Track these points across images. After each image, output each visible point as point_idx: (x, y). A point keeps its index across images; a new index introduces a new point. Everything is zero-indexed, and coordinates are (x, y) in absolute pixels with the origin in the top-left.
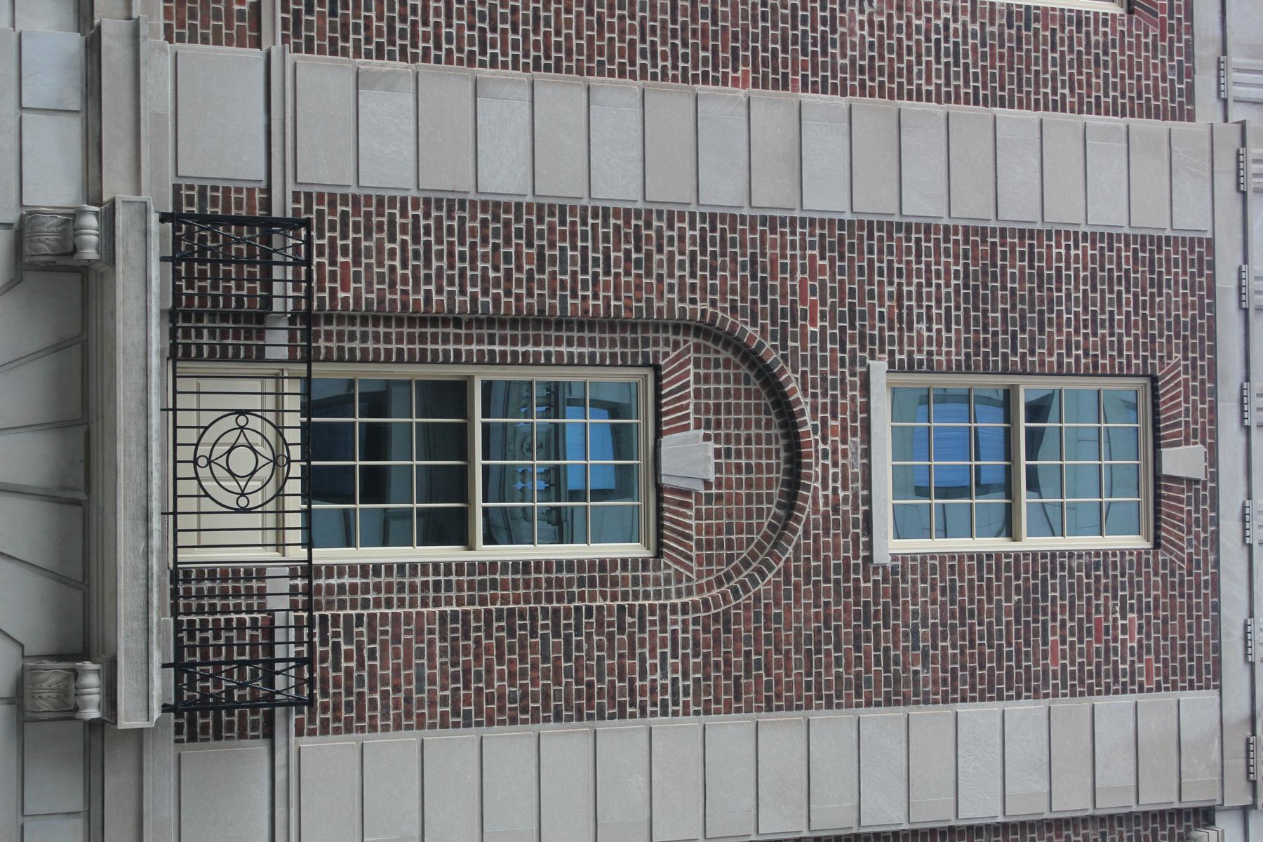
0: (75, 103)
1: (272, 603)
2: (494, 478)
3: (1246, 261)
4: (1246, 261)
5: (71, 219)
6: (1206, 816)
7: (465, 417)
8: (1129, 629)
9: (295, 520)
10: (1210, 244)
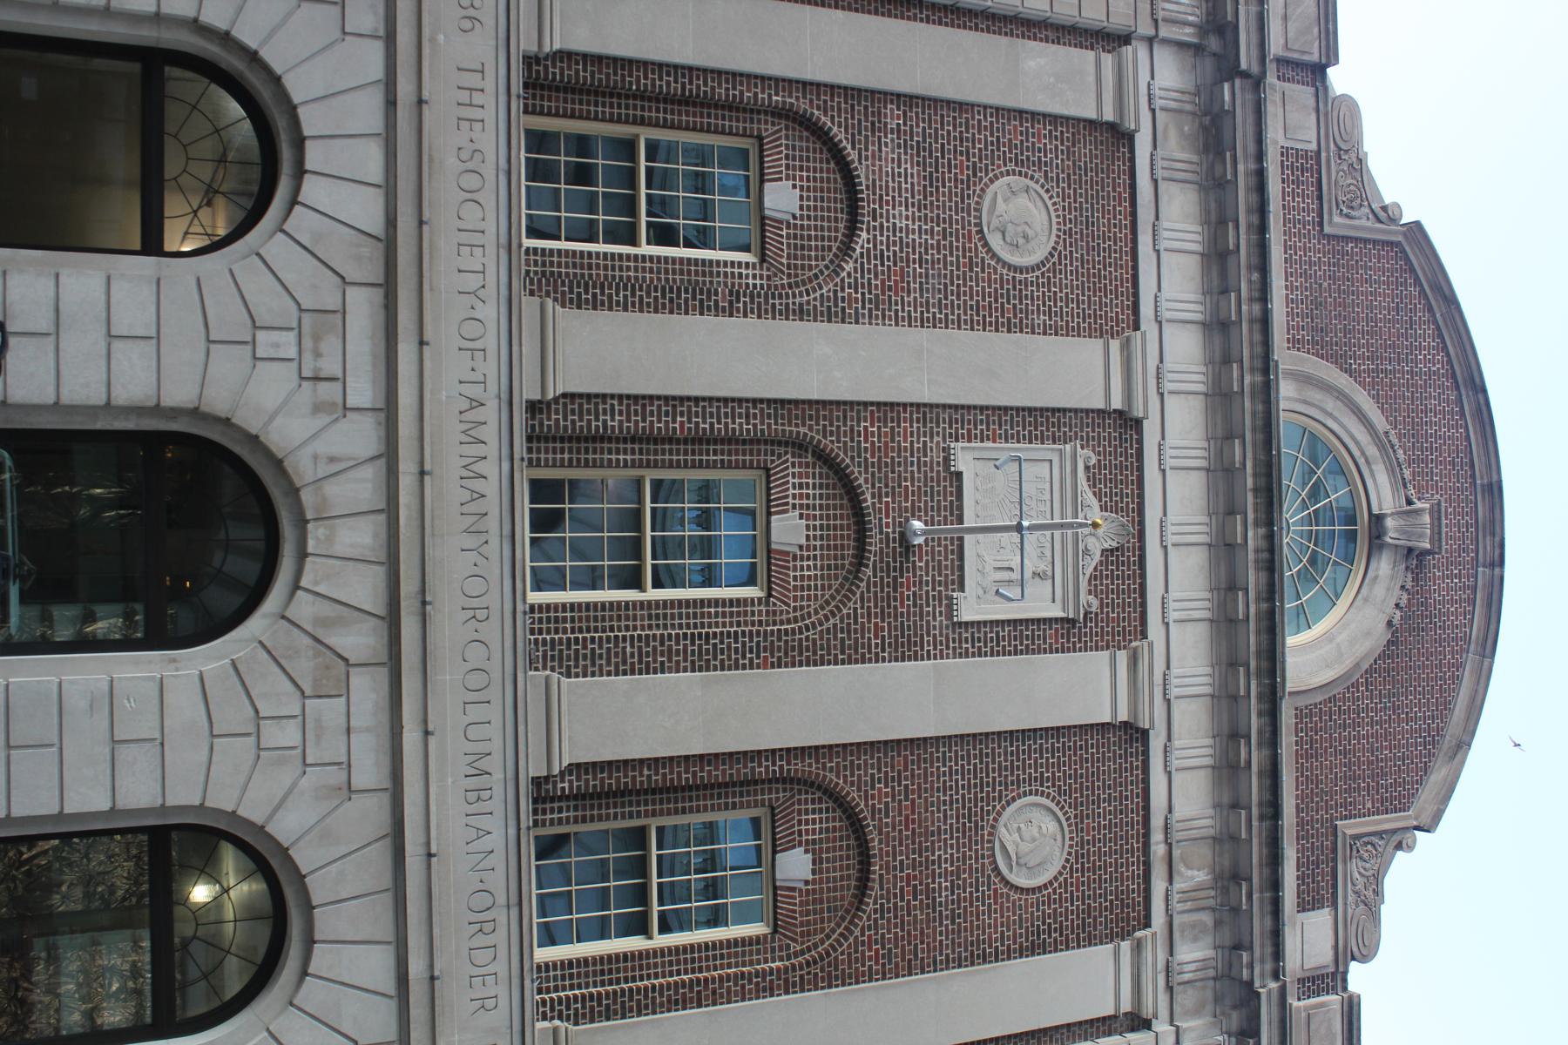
6: (1125, 39)
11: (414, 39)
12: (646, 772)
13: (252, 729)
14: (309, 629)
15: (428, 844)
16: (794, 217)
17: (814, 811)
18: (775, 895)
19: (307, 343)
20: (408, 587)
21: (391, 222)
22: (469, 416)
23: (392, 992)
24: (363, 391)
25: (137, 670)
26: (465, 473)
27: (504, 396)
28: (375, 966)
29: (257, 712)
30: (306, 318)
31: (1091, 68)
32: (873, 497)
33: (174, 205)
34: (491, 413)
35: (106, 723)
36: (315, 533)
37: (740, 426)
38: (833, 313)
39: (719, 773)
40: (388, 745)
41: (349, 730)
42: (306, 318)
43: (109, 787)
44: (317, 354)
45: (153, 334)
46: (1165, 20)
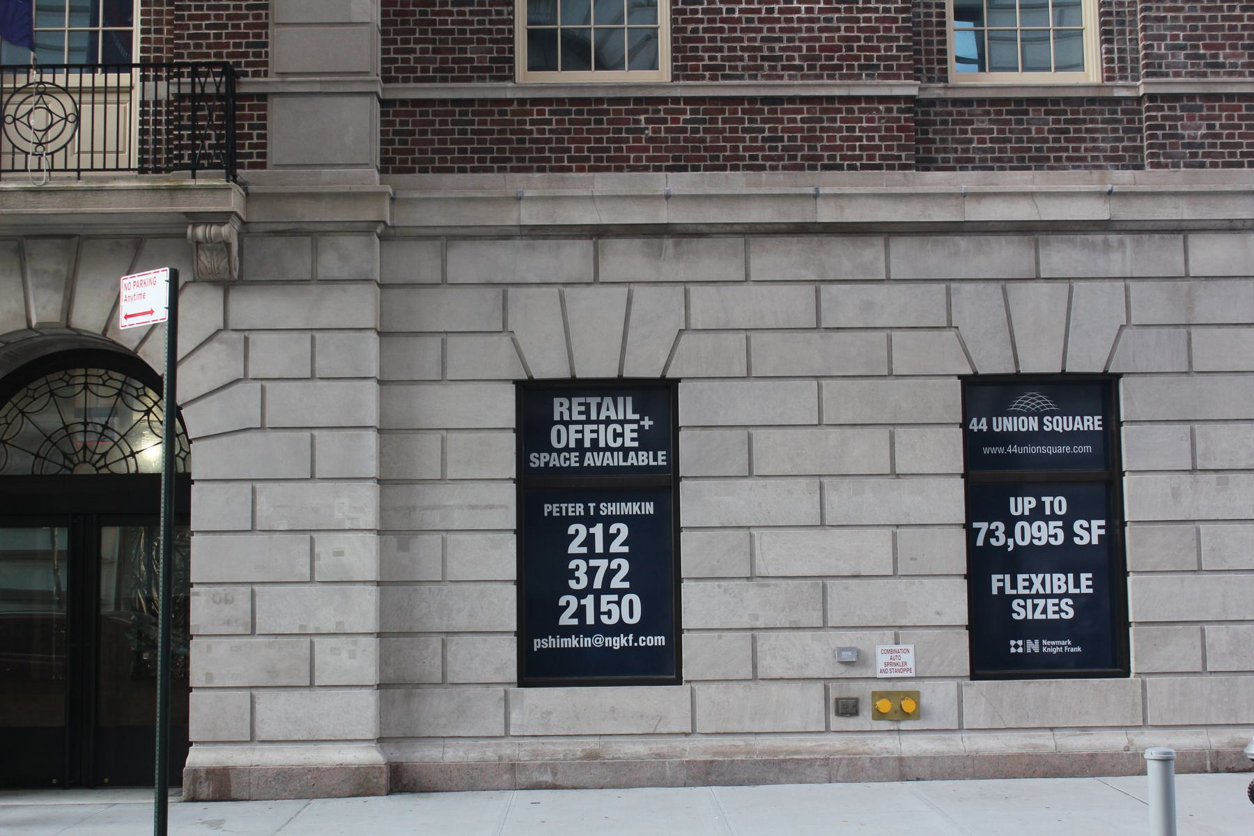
1: (162, 95)
9: (112, 79)
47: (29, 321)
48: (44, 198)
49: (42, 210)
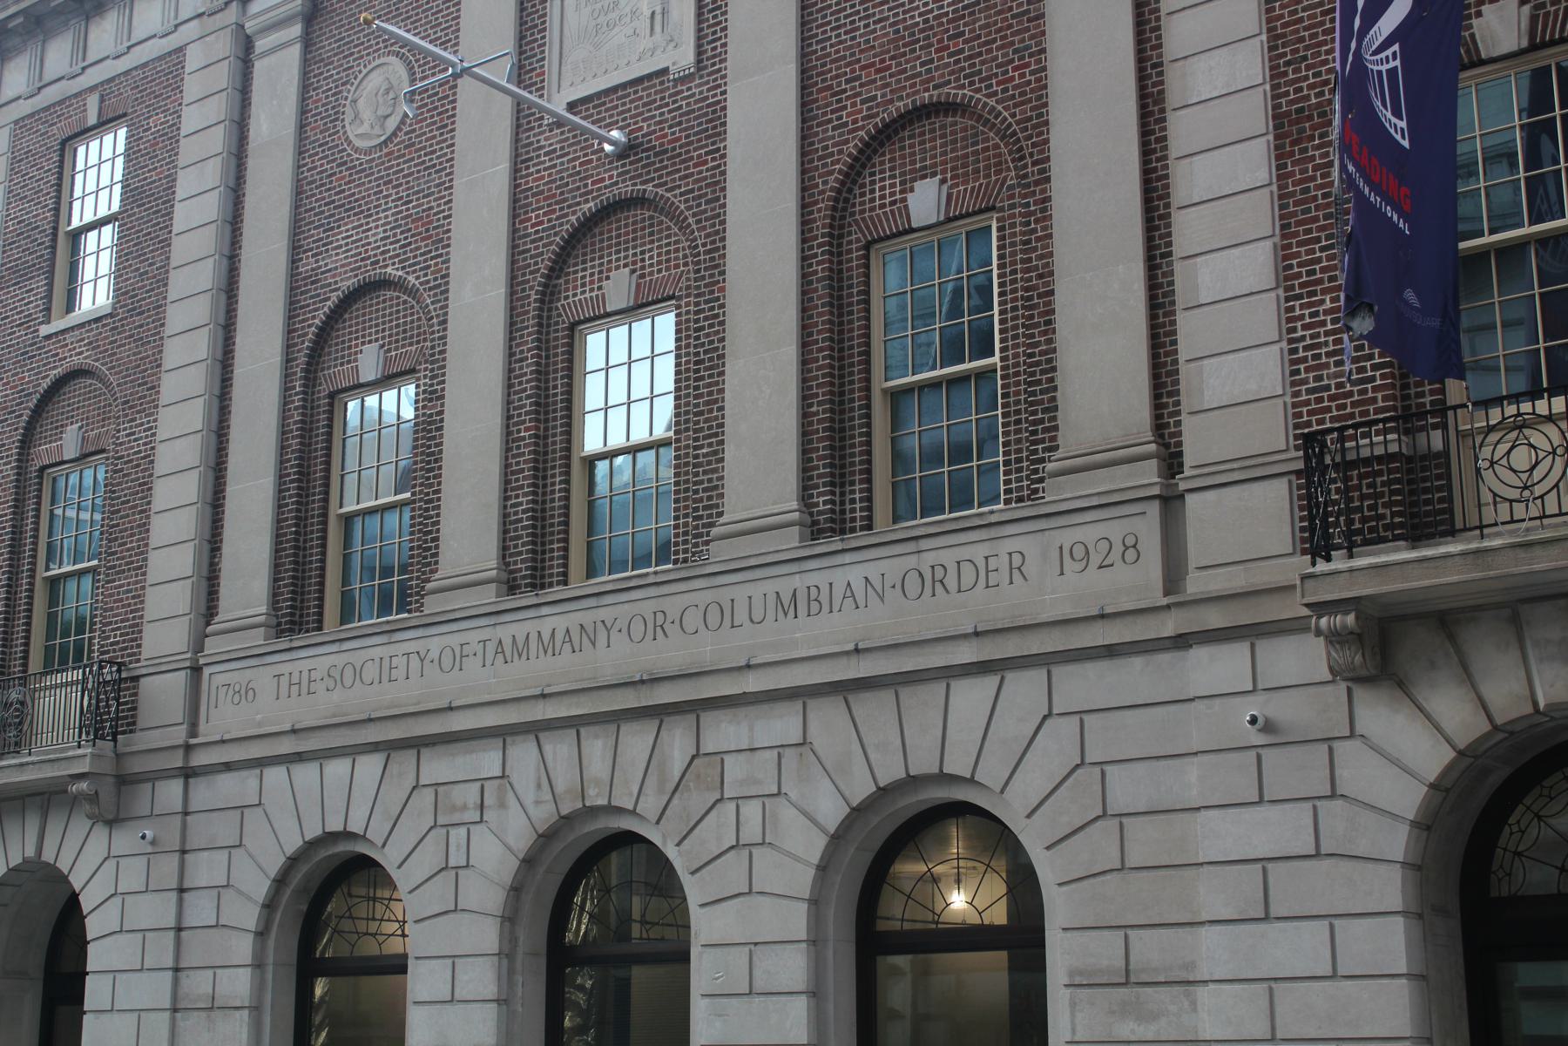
0: (799, 705)
2: (1497, 224)
3: (19, 98)
4: (19, 98)
5: (1335, 638)
7: (1488, 253)
8: (156, 122)
10: (16, 122)
11: (258, 741)
12: (814, 409)
13: (746, 852)
14: (666, 798)
15: (847, 653)
16: (382, 346)
17: (872, 191)
18: (956, 218)
19: (456, 818)
20: (630, 700)
21: (374, 747)
22: (508, 654)
23: (996, 679)
24: (487, 761)
25: (704, 971)
26: (524, 656)
27: (493, 620)
28: (971, 696)
29: (732, 847)
30: (441, 821)
31: (273, 58)
32: (587, 201)
33: (369, 948)
34: (508, 631)
35: (734, 1001)
36: (597, 798)
37: (528, 368)
38: (442, 289)
39: (821, 319)
40: (765, 707)
41: (752, 750)
42: (441, 821)
43: (789, 998)
44: (465, 807)
45: (449, 961)
46: (41, 79)
47: (1535, 704)
48: (1538, 551)
49: (1536, 567)
